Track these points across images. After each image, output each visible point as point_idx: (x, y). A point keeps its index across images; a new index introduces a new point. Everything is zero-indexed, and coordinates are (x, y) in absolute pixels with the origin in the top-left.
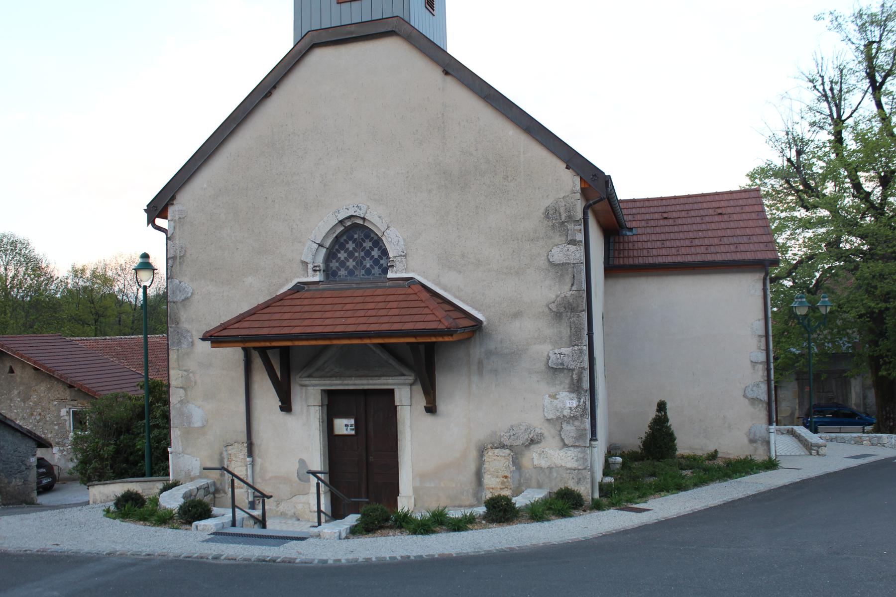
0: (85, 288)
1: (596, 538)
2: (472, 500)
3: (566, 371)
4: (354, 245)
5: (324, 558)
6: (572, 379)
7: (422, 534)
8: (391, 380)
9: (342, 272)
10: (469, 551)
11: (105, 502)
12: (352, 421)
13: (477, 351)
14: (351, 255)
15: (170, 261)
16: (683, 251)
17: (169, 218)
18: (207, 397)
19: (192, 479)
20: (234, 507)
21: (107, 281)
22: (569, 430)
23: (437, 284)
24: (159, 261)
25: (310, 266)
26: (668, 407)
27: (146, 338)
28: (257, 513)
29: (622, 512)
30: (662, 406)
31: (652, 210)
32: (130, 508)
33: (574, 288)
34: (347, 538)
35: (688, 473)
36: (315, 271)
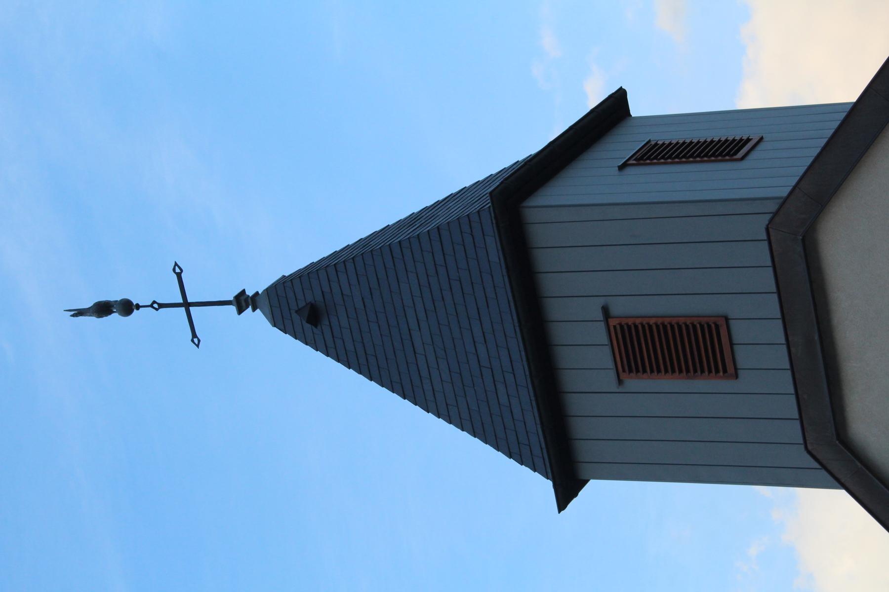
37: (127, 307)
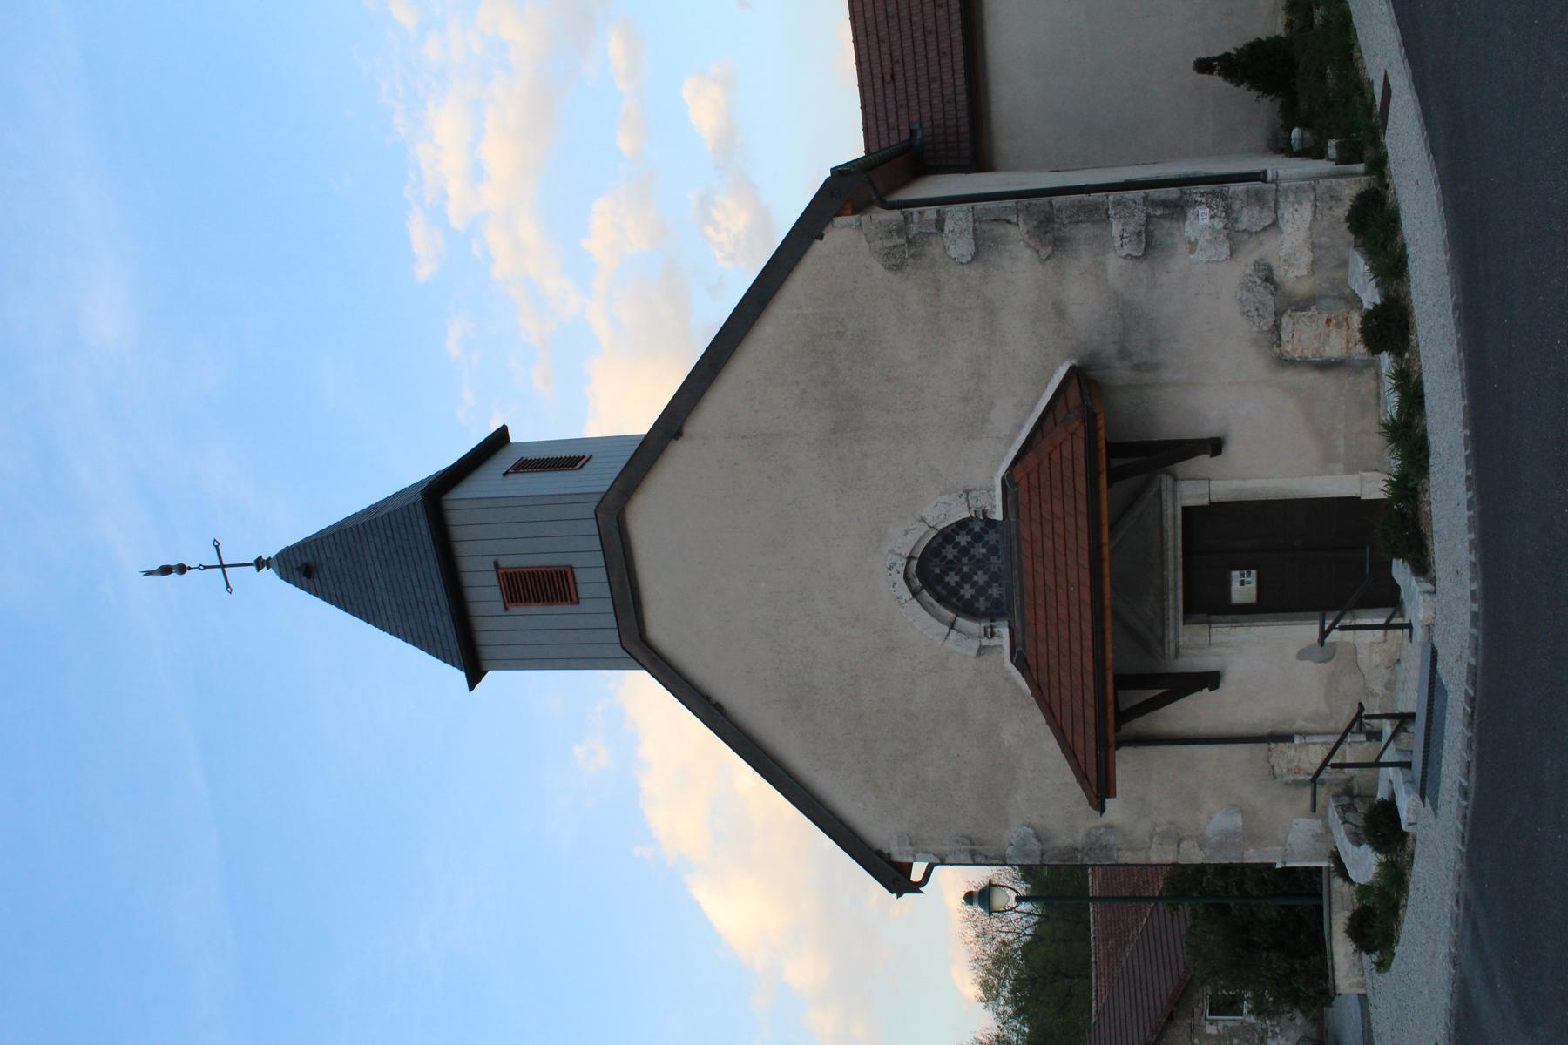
0: (1012, 992)
1: (1437, 164)
2: (1368, 376)
3: (1151, 228)
4: (952, 574)
5: (1468, 617)
6: (1163, 217)
7: (1427, 457)
8: (1169, 512)
9: (995, 591)
10: (1458, 377)
11: (1362, 969)
12: (1236, 574)
13: (1120, 374)
14: (966, 578)
15: (978, 860)
16: (944, 45)
17: (910, 860)
18: (1192, 805)
19: (1328, 830)
20: (1377, 764)
21: (1002, 959)
22: (1248, 218)
23: (1012, 439)
24: (977, 876)
25: (985, 642)
26: (1204, 55)
27: (1094, 899)
28: (1387, 727)
29: (1390, 122)
30: (1203, 66)
31: (880, 100)
32: (1376, 927)
33: (1013, 219)
34: (1433, 581)
35: (1318, 15)
36: (993, 634)
37: (182, 569)
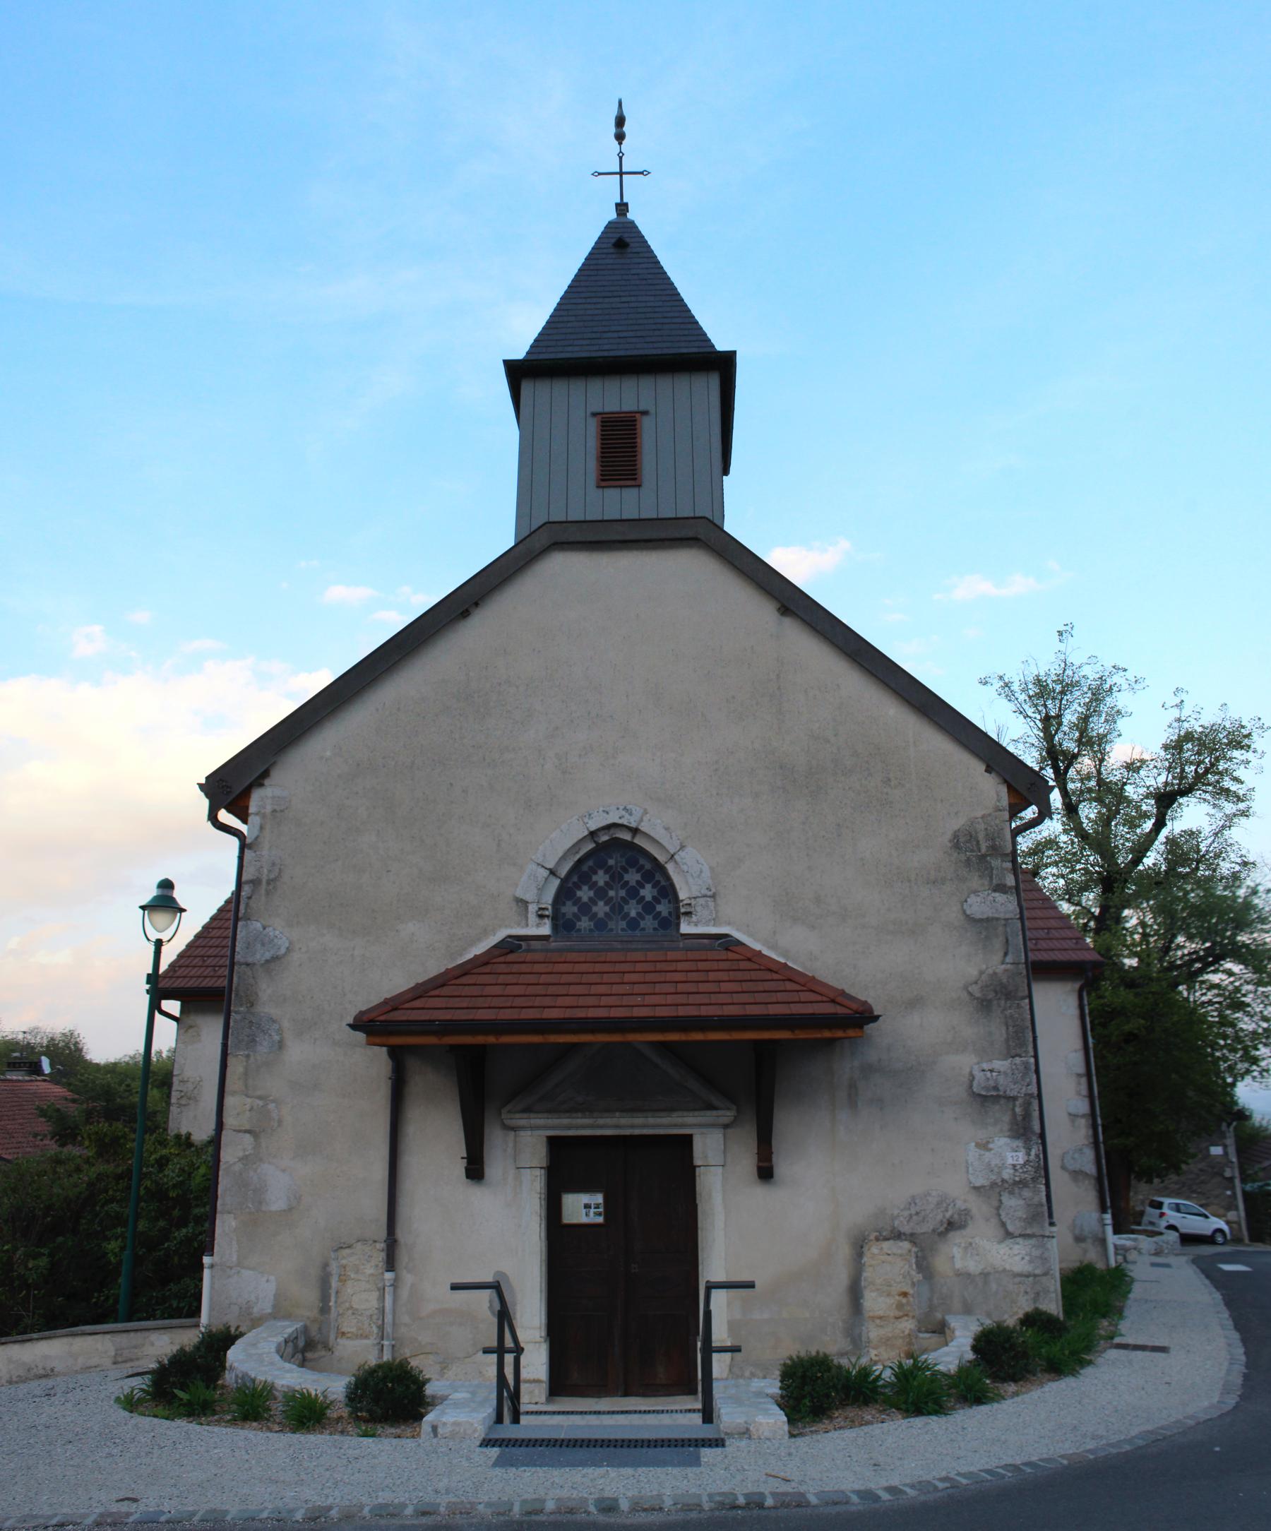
3: (1003, 1101)
4: (607, 878)
6: (1014, 1115)
8: (691, 1118)
13: (846, 1067)
14: (601, 893)
22: (1014, 1205)
